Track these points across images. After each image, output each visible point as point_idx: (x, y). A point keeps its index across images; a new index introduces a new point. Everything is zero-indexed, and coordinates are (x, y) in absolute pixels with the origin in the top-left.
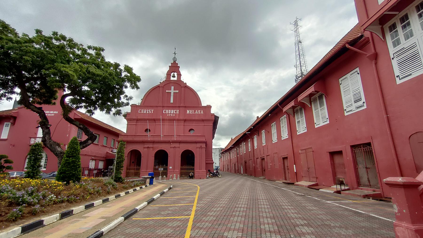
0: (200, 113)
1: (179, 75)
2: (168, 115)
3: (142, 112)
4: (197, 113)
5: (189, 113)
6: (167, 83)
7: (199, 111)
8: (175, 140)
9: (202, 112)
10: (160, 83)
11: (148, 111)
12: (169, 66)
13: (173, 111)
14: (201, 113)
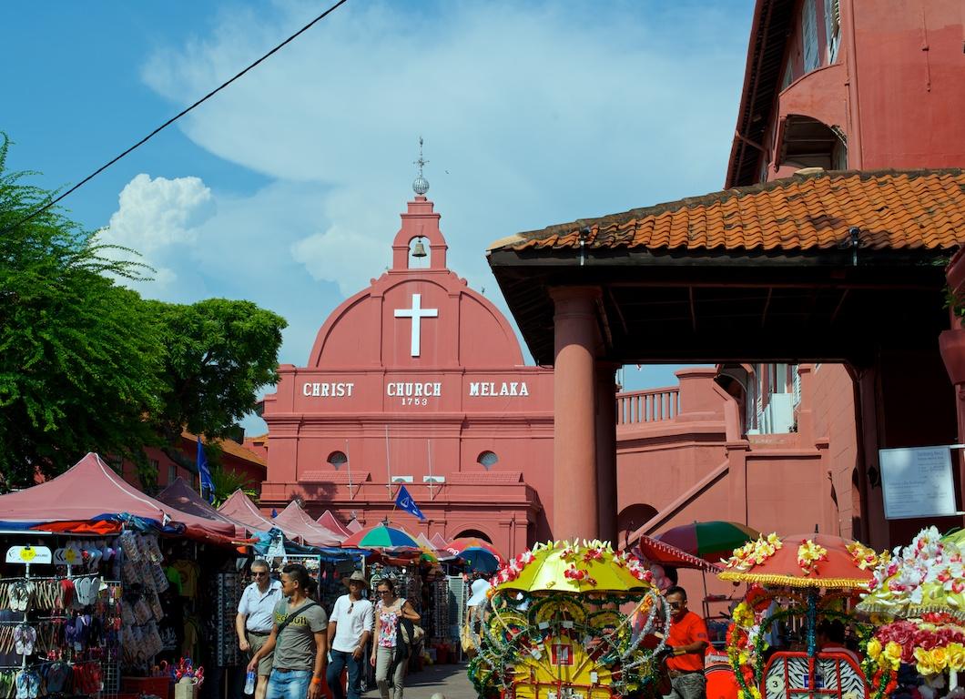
1: (440, 248)
2: (404, 400)
3: (316, 392)
6: (396, 284)
9: (524, 390)
11: (334, 390)
12: (403, 216)
13: (421, 388)
14: (521, 394)
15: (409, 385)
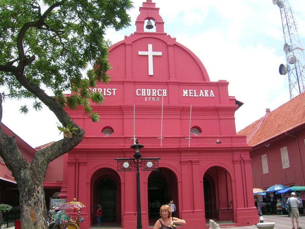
0: (208, 96)
1: (160, 24)
2: (146, 98)
4: (203, 96)
8: (189, 147)
9: (212, 94)
10: (126, 37)
13: (156, 92)
14: (211, 96)
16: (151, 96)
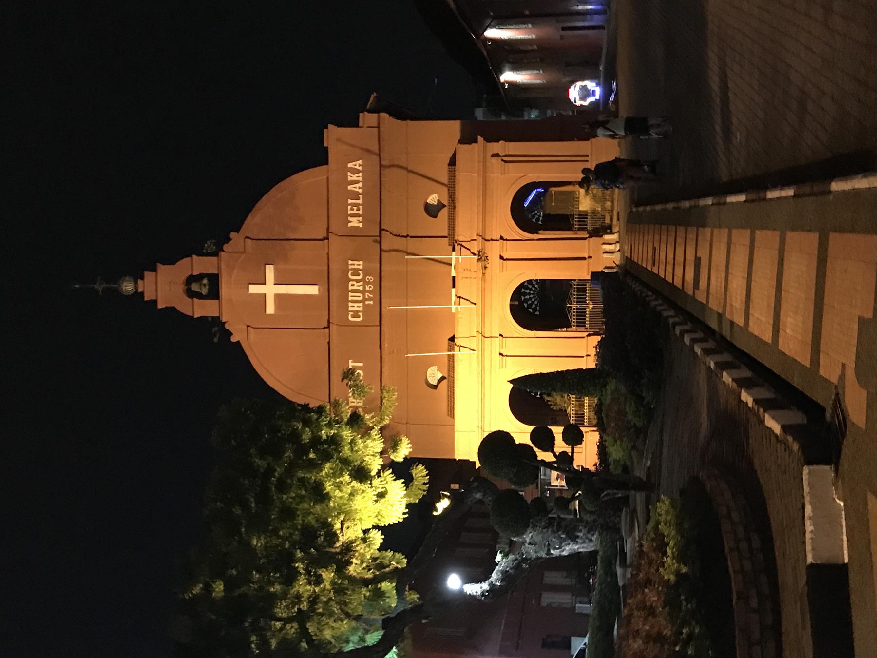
4: (360, 185)
5: (360, 219)
7: (352, 177)
9: (357, 165)
13: (354, 283)
14: (360, 168)
15: (351, 296)
16: (363, 292)
